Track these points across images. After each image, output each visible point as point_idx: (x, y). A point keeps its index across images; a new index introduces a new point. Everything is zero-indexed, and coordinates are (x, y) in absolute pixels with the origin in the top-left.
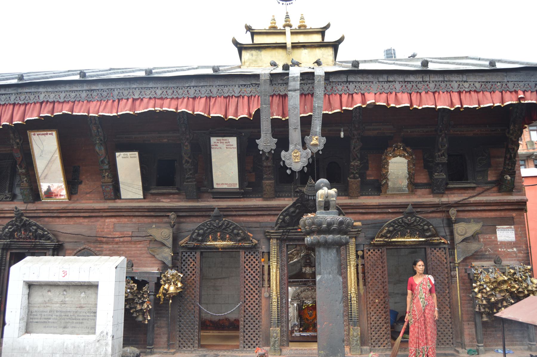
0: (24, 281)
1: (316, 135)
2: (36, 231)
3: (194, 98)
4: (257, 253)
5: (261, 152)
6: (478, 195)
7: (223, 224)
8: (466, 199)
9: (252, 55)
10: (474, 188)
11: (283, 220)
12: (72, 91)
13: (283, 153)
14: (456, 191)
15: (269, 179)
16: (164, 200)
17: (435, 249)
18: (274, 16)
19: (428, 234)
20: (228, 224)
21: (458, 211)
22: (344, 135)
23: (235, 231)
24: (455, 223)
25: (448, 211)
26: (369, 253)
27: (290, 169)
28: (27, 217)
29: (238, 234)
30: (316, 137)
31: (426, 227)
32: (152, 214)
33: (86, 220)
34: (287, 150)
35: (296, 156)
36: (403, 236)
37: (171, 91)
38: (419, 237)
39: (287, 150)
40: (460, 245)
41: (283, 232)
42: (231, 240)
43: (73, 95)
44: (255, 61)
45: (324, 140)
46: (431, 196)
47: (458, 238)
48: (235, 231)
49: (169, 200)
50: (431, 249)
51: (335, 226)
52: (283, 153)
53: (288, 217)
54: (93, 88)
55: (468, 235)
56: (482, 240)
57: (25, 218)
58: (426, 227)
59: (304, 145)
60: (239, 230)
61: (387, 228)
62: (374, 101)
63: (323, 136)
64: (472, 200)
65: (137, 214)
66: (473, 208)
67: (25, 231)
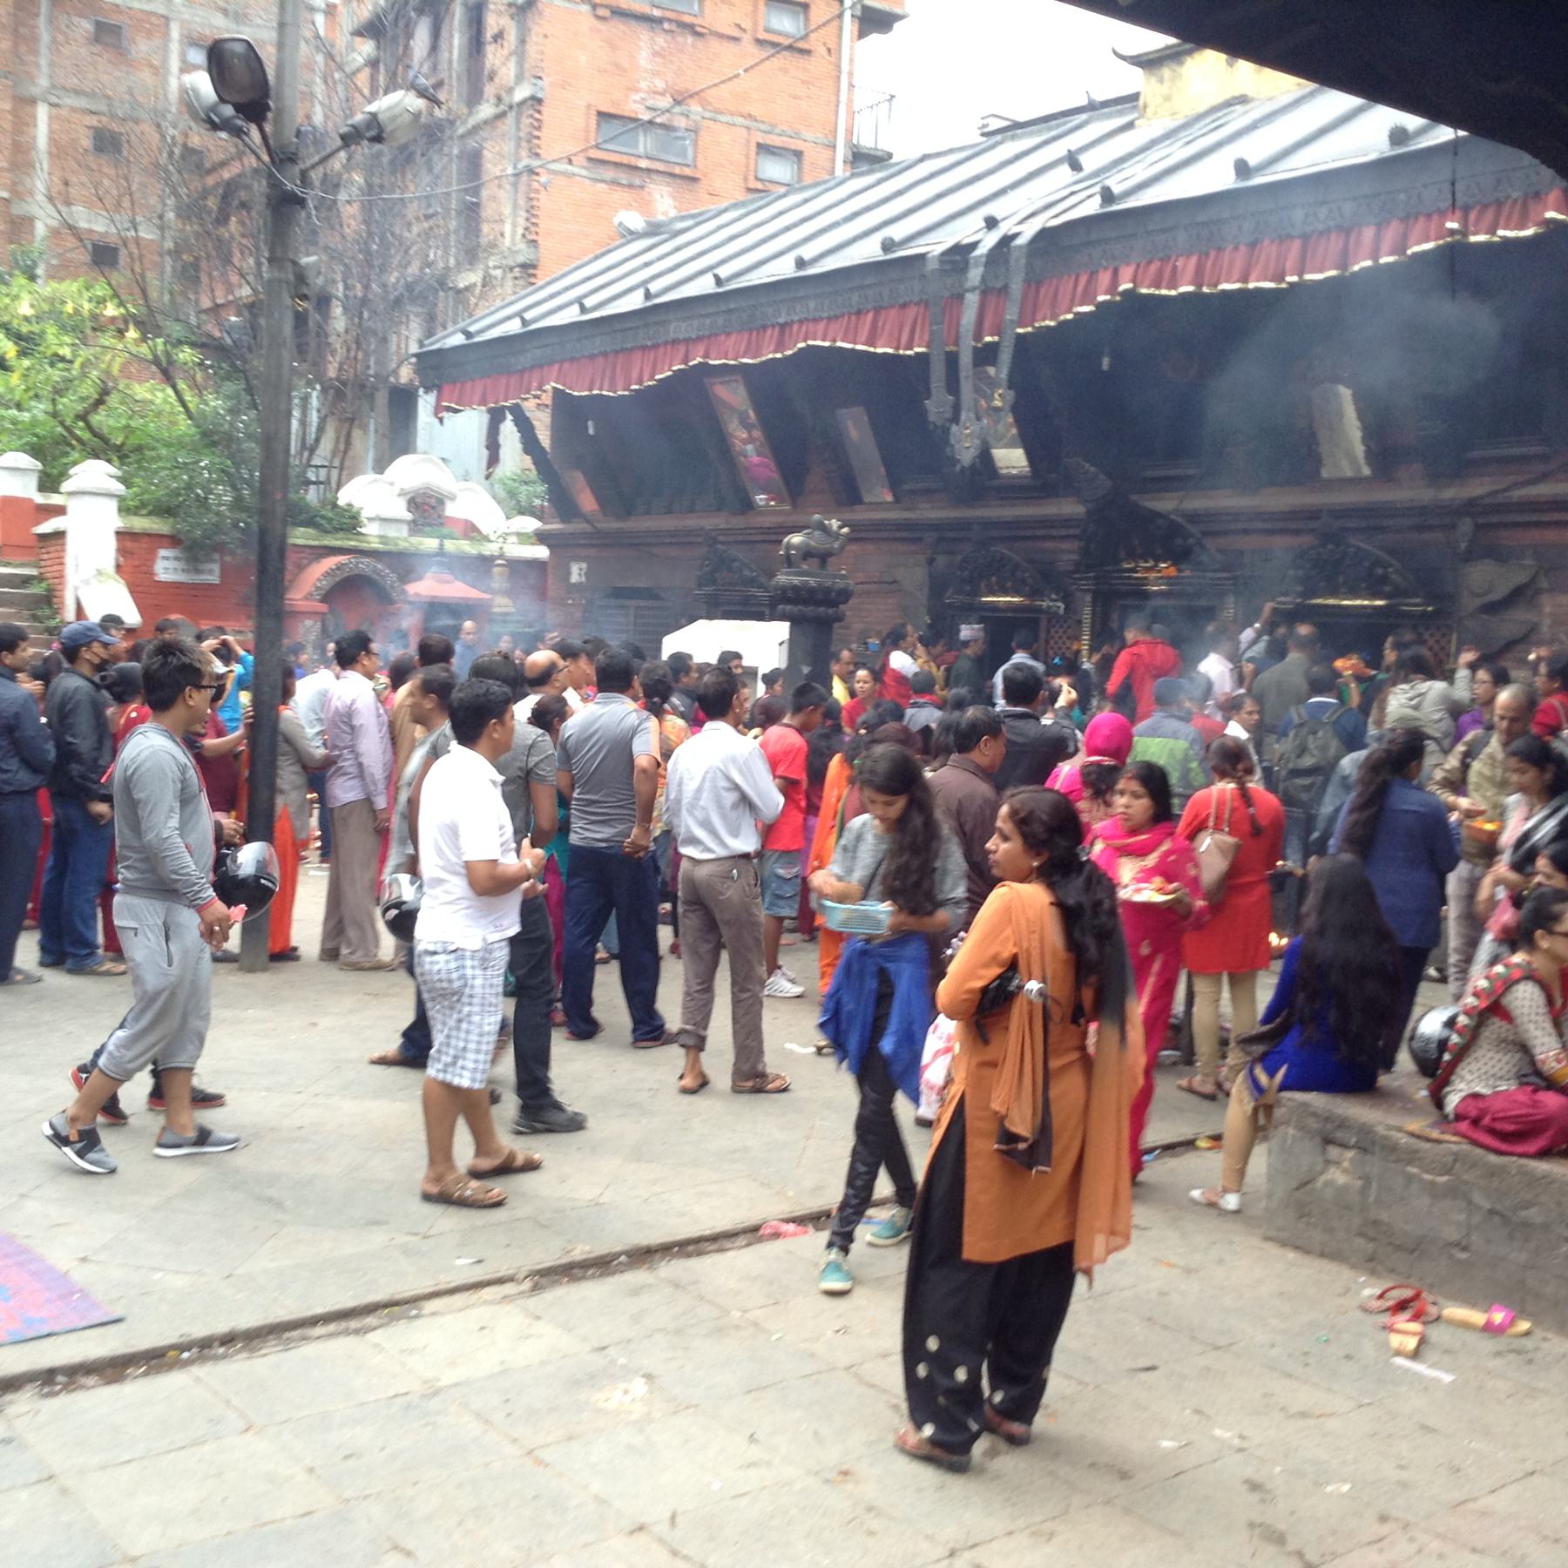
2: (741, 571)
3: (859, 313)
6: (1543, 477)
8: (1497, 492)
10: (1544, 458)
13: (954, 428)
17: (1427, 629)
19: (1387, 589)
22: (1111, 365)
23: (1019, 574)
24: (1467, 560)
25: (1454, 526)
28: (723, 543)
31: (1380, 571)
32: (905, 534)
36: (1334, 594)
37: (826, 302)
40: (1470, 623)
41: (1096, 578)
42: (1016, 593)
43: (708, 321)
44: (1167, 98)
45: (1011, 395)
49: (928, 506)
53: (1092, 545)
54: (732, 306)
55: (1496, 596)
56: (1547, 609)
57: (719, 547)
62: (1130, 285)
63: (1010, 388)
64: (1518, 494)
67: (730, 569)
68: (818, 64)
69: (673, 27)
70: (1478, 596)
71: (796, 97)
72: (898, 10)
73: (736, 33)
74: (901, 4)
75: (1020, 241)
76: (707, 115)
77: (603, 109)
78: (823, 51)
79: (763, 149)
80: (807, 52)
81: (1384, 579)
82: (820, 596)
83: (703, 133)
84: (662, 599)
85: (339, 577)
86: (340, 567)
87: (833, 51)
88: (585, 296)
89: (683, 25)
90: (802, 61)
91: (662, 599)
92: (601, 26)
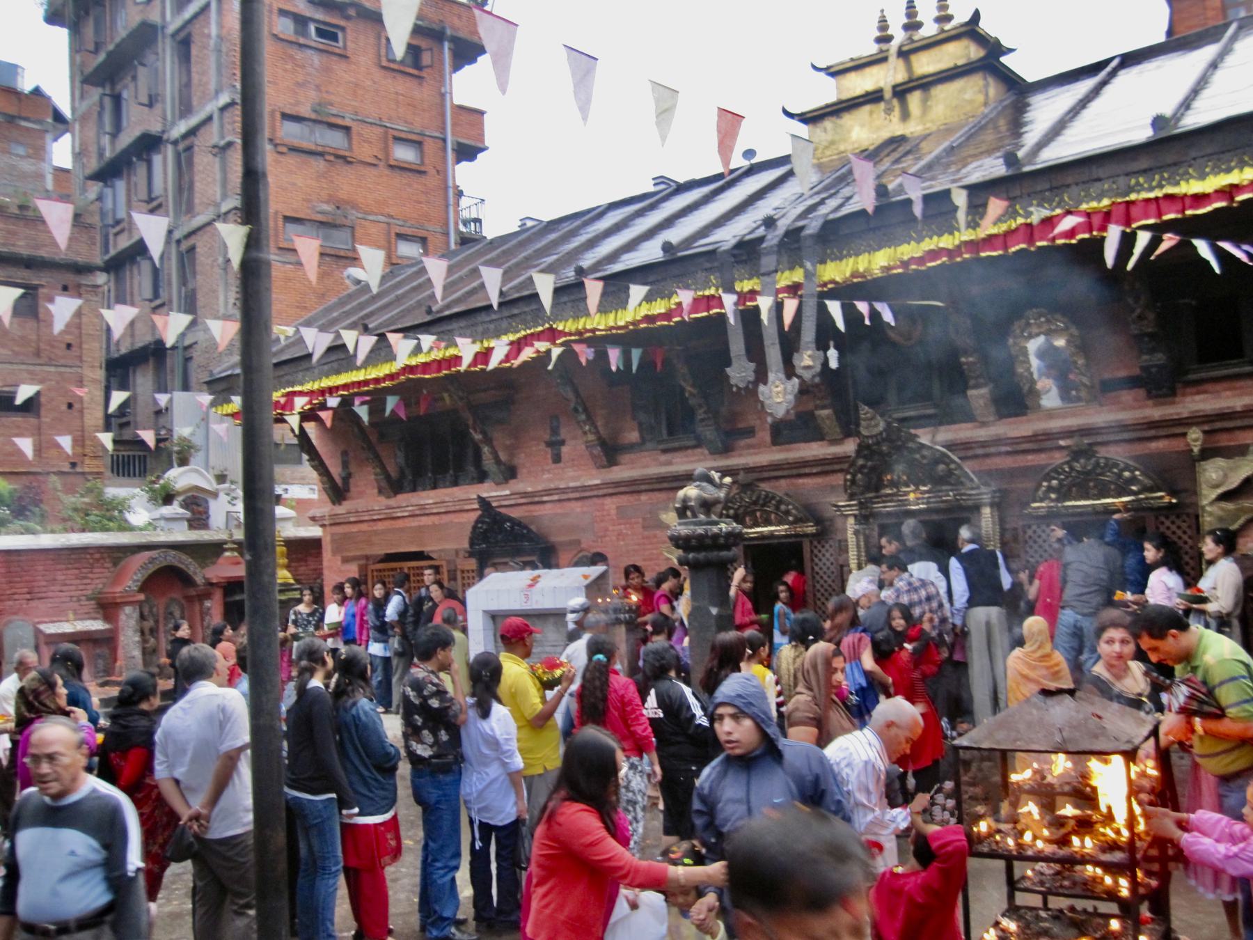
0: (485, 612)
1: (808, 349)
4: (831, 542)
5: (734, 389)
7: (759, 497)
9: (825, 130)
11: (853, 482)
12: (491, 321)
13: (762, 388)
14: (1209, 387)
15: (824, 407)
16: (678, 460)
18: (882, 11)
20: (767, 496)
21: (1205, 432)
23: (783, 507)
25: (1184, 435)
26: (1030, 532)
27: (771, 414)
29: (787, 513)
30: (809, 352)
31: (1127, 474)
33: (579, 504)
34: (765, 383)
35: (778, 393)
38: (1120, 495)
39: (765, 383)
46: (1150, 402)
47: (1208, 496)
48: (783, 507)
50: (1157, 518)
51: (694, 542)
52: (762, 388)
54: (516, 311)
58: (1127, 474)
59: (790, 372)
60: (788, 505)
61: (1045, 484)
65: (643, 487)
66: (1239, 423)
68: (432, 180)
69: (332, 158)
70: (1217, 486)
71: (420, 203)
72: (480, 145)
73: (374, 161)
74: (483, 141)
75: (808, 232)
76: (360, 215)
77: (288, 214)
78: (434, 172)
79: (400, 236)
80: (424, 172)
81: (1133, 480)
82: (722, 541)
83: (357, 228)
84: (431, 559)
85: (152, 568)
86: (152, 560)
87: (442, 173)
88: (368, 316)
89: (338, 157)
90: (423, 179)
91: (431, 559)
92: (281, 158)
